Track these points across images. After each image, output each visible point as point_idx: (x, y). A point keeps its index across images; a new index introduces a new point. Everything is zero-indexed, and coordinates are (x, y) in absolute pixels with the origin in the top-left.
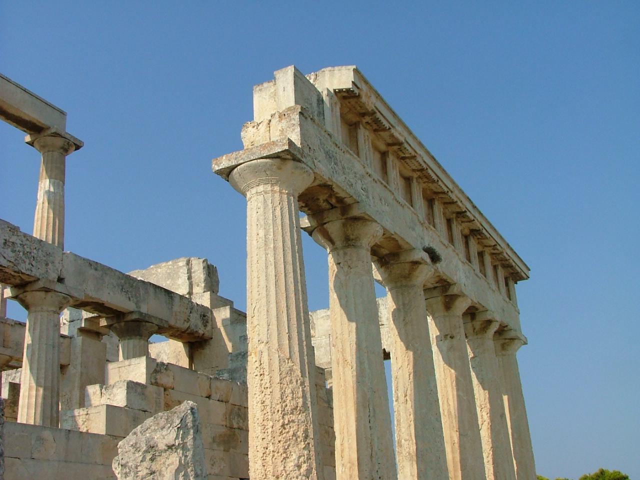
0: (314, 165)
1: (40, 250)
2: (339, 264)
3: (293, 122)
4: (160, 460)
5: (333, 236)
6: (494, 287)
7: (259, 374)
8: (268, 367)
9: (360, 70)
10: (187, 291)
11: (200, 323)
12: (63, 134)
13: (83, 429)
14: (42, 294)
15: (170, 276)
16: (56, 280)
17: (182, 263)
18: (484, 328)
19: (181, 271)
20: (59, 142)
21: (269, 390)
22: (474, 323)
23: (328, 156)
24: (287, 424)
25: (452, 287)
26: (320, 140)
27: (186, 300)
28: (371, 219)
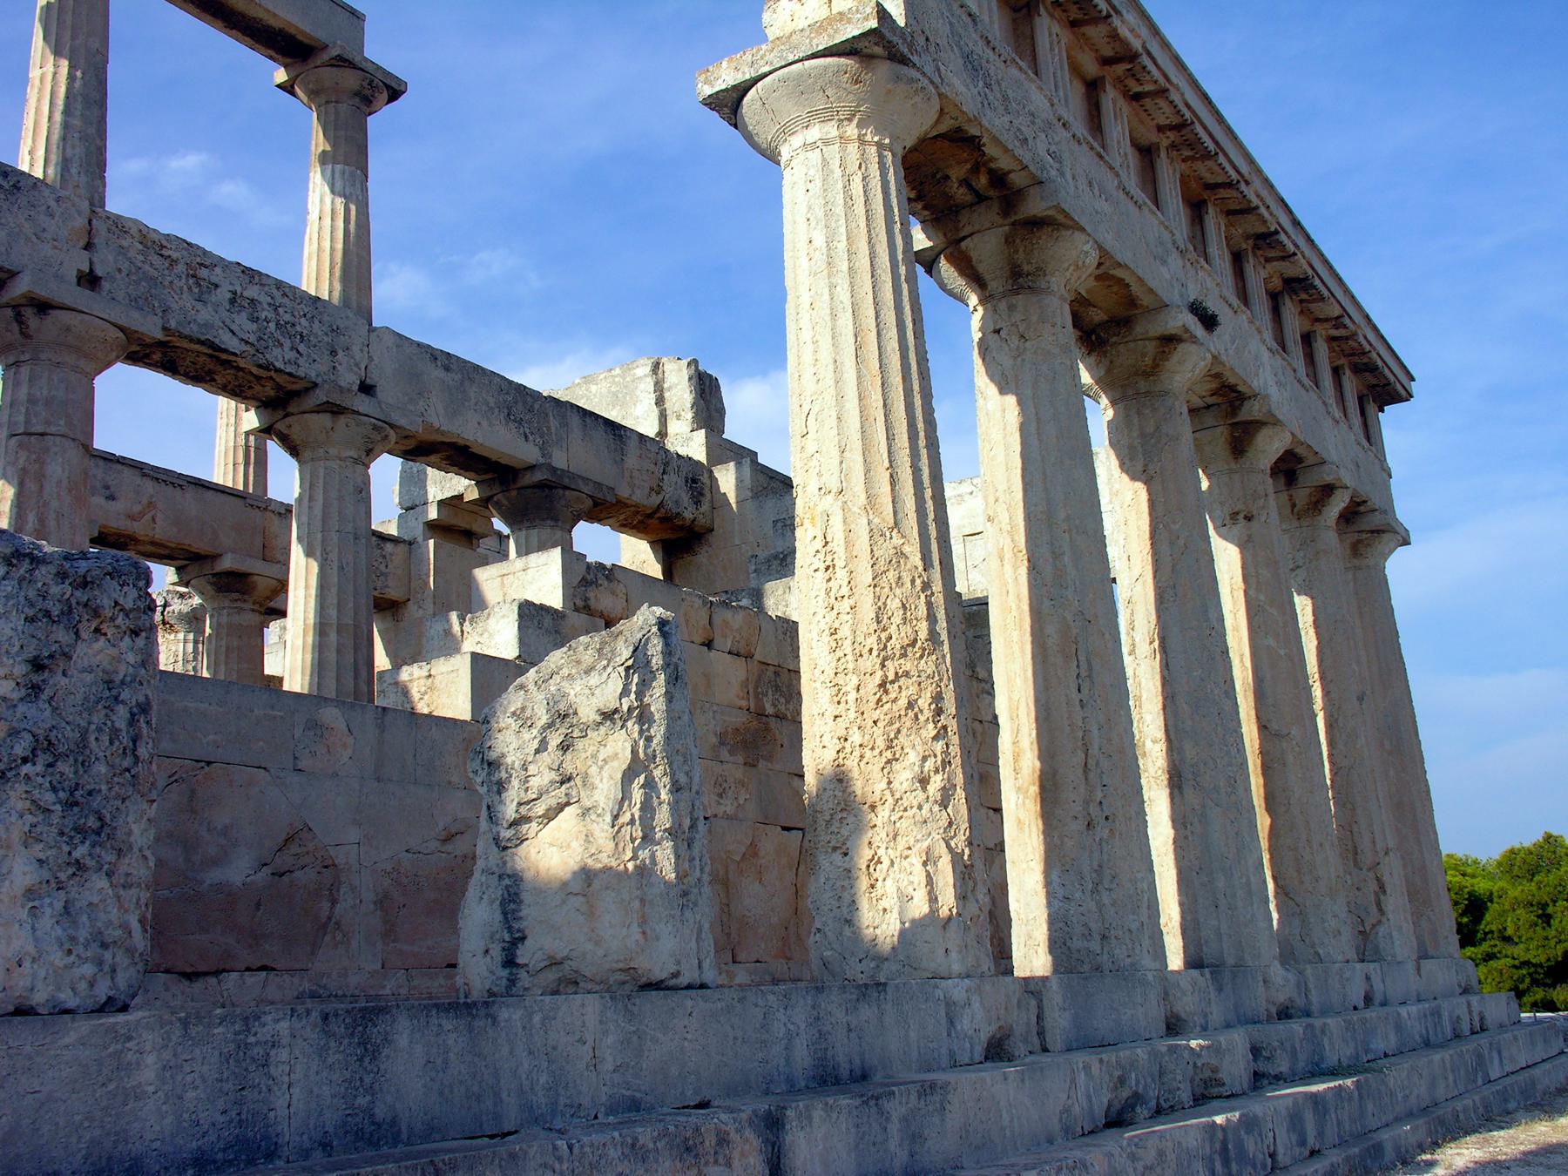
0: (940, 76)
1: (316, 322)
2: (998, 331)
4: (585, 747)
5: (981, 268)
6: (1338, 414)
7: (822, 567)
8: (843, 549)
10: (656, 429)
11: (685, 498)
13: (422, 708)
14: (325, 419)
15: (616, 399)
16: (355, 388)
17: (643, 369)
18: (1318, 502)
19: (642, 386)
20: (350, 80)
21: (846, 604)
22: (1292, 492)
23: (970, 66)
24: (892, 682)
25: (1247, 405)
26: (951, 24)
27: (654, 447)
28: (1071, 223)
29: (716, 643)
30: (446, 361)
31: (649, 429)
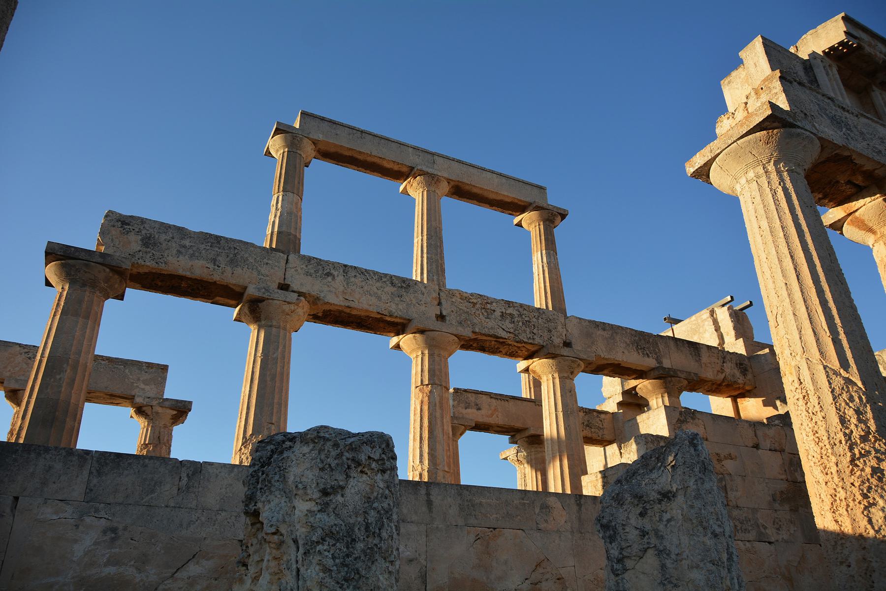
0: (816, 129)
1: (540, 319)
3: (774, 91)
7: (801, 396)
8: (811, 384)
9: (852, 15)
11: (737, 373)
12: (545, 206)
15: (695, 331)
16: (561, 345)
17: (705, 314)
21: (820, 416)
23: (835, 122)
24: (859, 459)
26: (818, 105)
27: (719, 353)
29: (761, 446)
30: (603, 326)
31: (714, 342)
